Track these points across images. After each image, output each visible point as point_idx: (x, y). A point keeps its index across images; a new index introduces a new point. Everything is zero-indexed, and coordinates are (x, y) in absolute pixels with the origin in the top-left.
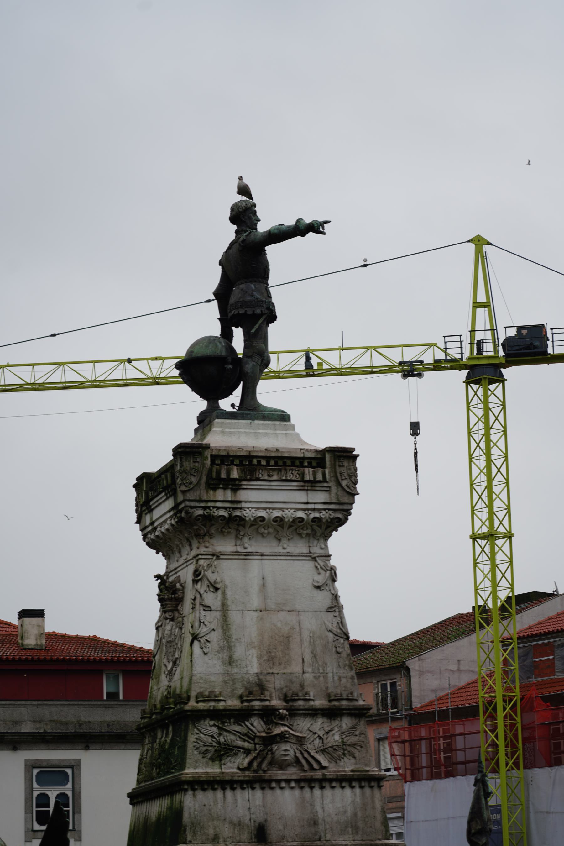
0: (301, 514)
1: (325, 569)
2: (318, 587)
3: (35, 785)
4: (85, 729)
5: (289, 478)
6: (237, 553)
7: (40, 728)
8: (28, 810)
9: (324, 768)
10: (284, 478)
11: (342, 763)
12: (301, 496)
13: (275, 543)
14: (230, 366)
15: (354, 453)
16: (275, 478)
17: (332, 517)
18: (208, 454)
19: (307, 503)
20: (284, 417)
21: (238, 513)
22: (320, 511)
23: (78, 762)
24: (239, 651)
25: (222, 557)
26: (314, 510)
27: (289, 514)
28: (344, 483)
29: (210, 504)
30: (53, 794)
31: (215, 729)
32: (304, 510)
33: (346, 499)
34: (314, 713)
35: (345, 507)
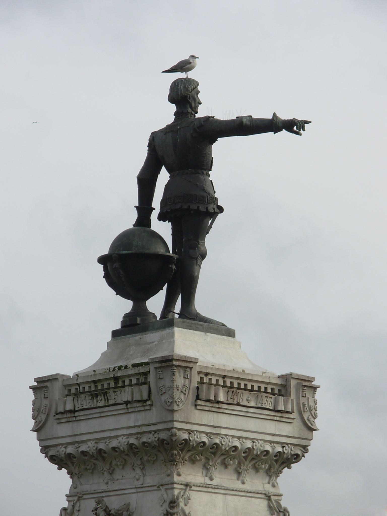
0: (268, 447)
1: (278, 510)
5: (264, 406)
6: (204, 486)
10: (259, 405)
13: (235, 477)
15: (313, 383)
16: (253, 404)
17: (293, 453)
18: (196, 368)
19: (274, 435)
20: (230, 333)
22: (283, 445)
25: (193, 488)
26: (278, 443)
27: (260, 446)
28: (305, 416)
29: (195, 428)
32: (271, 442)
33: (306, 433)
35: (304, 443)
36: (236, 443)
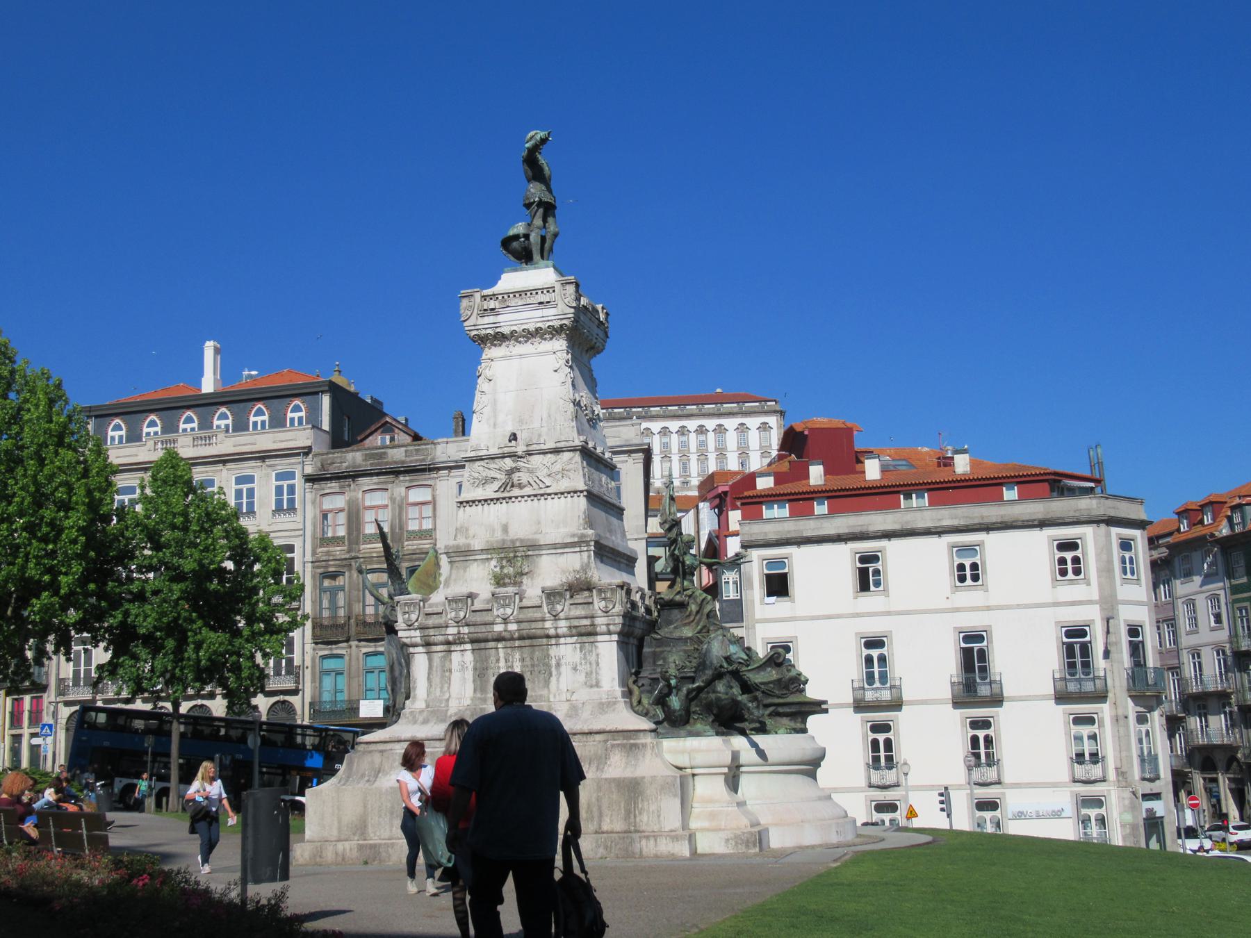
2: (556, 371)
3: (955, 558)
4: (986, 521)
7: (956, 522)
8: (952, 574)
9: (548, 487)
11: (560, 483)
12: (539, 313)
14: (523, 239)
21: (498, 330)
23: (983, 542)
24: (501, 418)
27: (532, 327)
30: (968, 563)
31: (481, 468)
34: (544, 452)
36: (514, 328)
